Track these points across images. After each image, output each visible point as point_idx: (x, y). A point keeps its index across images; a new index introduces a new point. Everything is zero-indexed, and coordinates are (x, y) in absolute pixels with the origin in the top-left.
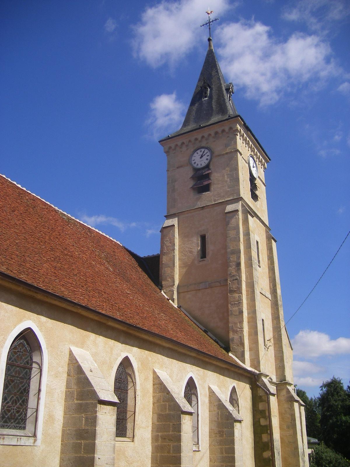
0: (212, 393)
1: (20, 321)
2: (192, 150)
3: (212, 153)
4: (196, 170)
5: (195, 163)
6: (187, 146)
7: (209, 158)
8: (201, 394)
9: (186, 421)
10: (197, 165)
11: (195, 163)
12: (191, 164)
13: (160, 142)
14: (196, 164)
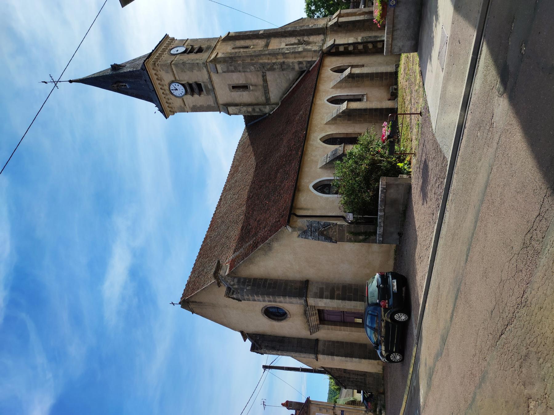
0: (335, 87)
1: (310, 191)
2: (171, 96)
3: (173, 82)
4: (186, 93)
5: (181, 94)
6: (168, 99)
7: (177, 84)
8: (336, 94)
9: (351, 106)
10: (183, 92)
11: (181, 94)
12: (183, 96)
13: (166, 118)
14: (182, 93)
